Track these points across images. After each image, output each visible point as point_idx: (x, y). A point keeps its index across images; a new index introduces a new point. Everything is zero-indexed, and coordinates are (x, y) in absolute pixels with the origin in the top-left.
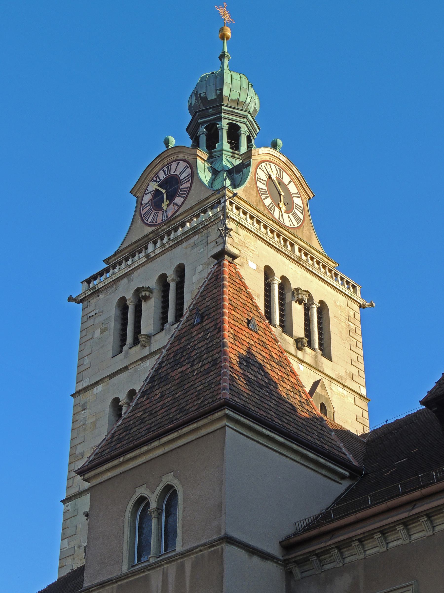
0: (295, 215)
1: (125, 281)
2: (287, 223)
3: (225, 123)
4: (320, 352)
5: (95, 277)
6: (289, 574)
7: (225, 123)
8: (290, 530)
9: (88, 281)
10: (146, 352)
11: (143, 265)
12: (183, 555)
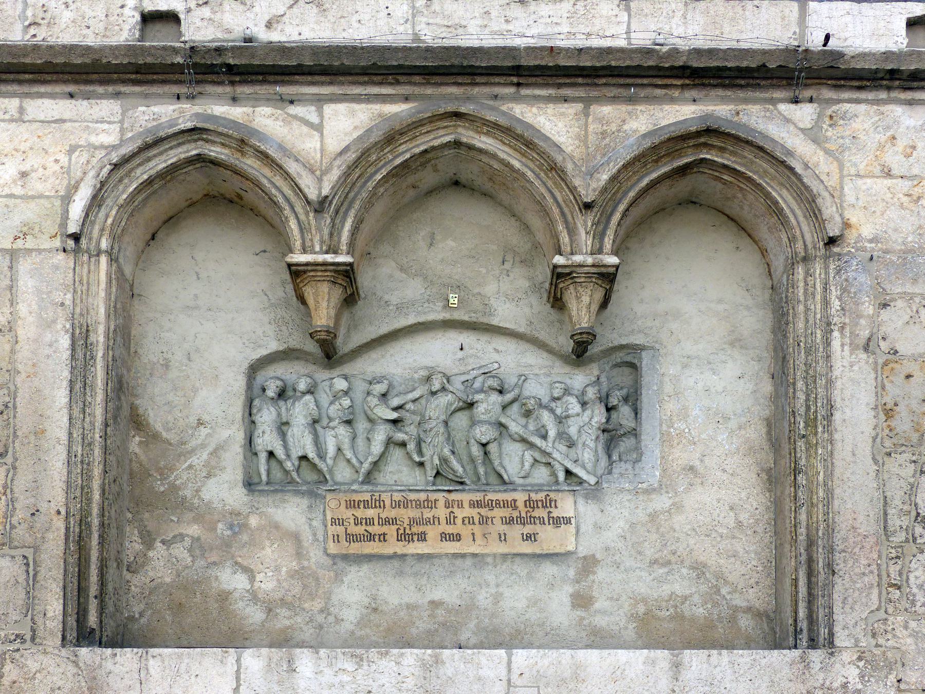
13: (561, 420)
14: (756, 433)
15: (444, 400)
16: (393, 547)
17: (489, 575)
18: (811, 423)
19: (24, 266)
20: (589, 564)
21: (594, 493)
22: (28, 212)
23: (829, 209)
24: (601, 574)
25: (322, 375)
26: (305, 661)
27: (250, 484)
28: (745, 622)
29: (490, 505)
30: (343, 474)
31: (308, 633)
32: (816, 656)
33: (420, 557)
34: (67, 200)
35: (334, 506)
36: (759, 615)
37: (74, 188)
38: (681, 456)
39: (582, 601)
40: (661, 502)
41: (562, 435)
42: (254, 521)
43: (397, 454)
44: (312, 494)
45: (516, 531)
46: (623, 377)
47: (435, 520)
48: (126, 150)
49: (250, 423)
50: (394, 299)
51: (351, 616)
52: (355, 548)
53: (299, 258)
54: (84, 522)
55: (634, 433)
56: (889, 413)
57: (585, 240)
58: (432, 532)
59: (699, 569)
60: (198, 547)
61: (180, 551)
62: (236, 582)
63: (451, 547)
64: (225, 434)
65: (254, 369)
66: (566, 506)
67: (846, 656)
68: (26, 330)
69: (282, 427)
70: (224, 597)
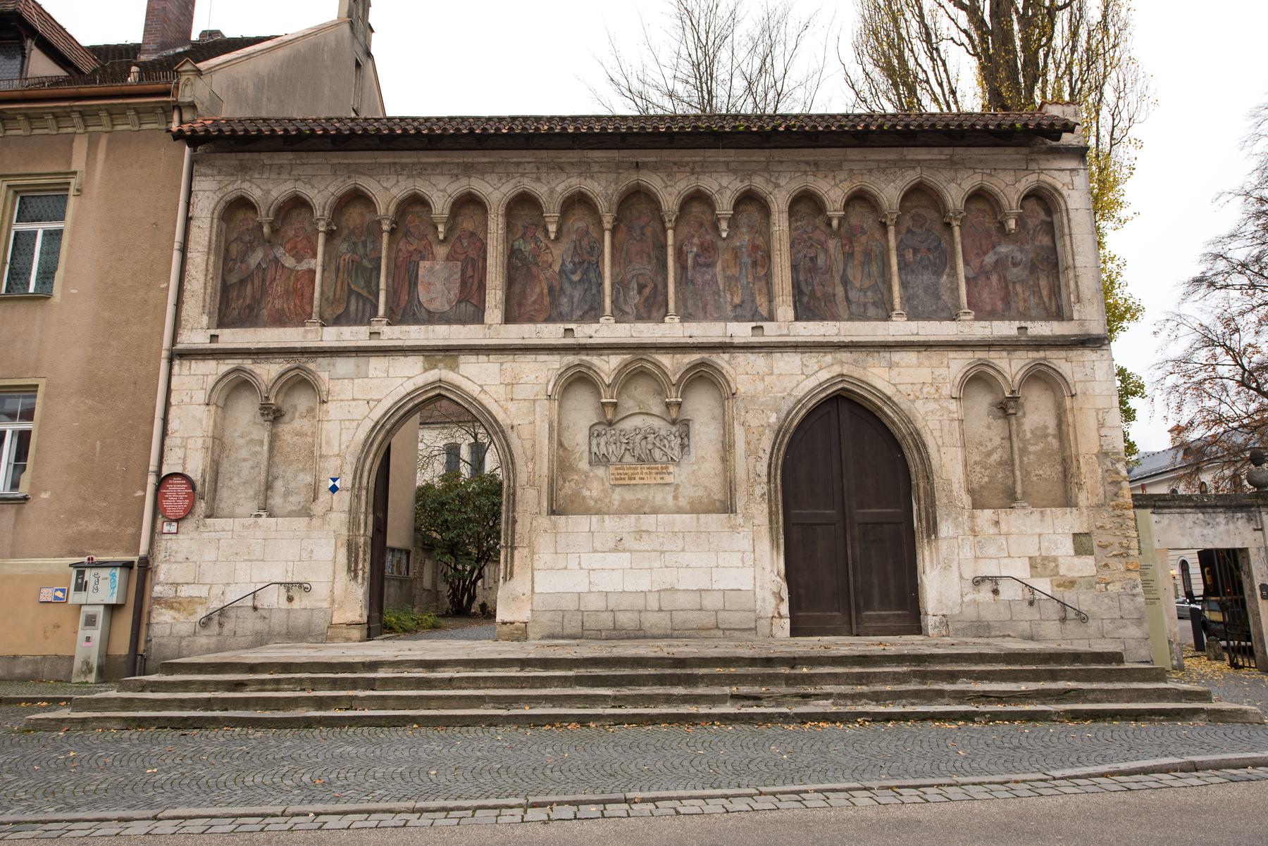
13: (669, 442)
14: (719, 446)
15: (639, 436)
16: (627, 482)
17: (652, 490)
18: (730, 446)
19: (537, 404)
20: (677, 486)
21: (678, 464)
22: (538, 388)
23: (733, 385)
24: (681, 489)
25: (608, 429)
26: (606, 517)
27: (590, 463)
28: (718, 504)
29: (652, 469)
30: (613, 459)
31: (605, 509)
32: (732, 515)
33: (634, 485)
34: (547, 384)
35: (612, 469)
36: (721, 502)
37: (549, 381)
39: (675, 498)
40: (695, 467)
41: (670, 446)
42: (591, 474)
43: (627, 452)
44: (606, 466)
45: (658, 477)
46: (685, 428)
47: (637, 474)
48: (562, 370)
49: (590, 444)
50: (626, 406)
51: (616, 503)
52: (617, 482)
53: (604, 400)
54: (553, 479)
55: (688, 446)
56: (749, 444)
57: (674, 394)
58: (637, 477)
59: (706, 487)
60: (577, 483)
61: (572, 484)
62: (586, 493)
63: (642, 482)
64: (583, 448)
65: (591, 428)
66: (671, 469)
67: (740, 516)
68: (538, 422)
69: (598, 444)
70: (584, 498)
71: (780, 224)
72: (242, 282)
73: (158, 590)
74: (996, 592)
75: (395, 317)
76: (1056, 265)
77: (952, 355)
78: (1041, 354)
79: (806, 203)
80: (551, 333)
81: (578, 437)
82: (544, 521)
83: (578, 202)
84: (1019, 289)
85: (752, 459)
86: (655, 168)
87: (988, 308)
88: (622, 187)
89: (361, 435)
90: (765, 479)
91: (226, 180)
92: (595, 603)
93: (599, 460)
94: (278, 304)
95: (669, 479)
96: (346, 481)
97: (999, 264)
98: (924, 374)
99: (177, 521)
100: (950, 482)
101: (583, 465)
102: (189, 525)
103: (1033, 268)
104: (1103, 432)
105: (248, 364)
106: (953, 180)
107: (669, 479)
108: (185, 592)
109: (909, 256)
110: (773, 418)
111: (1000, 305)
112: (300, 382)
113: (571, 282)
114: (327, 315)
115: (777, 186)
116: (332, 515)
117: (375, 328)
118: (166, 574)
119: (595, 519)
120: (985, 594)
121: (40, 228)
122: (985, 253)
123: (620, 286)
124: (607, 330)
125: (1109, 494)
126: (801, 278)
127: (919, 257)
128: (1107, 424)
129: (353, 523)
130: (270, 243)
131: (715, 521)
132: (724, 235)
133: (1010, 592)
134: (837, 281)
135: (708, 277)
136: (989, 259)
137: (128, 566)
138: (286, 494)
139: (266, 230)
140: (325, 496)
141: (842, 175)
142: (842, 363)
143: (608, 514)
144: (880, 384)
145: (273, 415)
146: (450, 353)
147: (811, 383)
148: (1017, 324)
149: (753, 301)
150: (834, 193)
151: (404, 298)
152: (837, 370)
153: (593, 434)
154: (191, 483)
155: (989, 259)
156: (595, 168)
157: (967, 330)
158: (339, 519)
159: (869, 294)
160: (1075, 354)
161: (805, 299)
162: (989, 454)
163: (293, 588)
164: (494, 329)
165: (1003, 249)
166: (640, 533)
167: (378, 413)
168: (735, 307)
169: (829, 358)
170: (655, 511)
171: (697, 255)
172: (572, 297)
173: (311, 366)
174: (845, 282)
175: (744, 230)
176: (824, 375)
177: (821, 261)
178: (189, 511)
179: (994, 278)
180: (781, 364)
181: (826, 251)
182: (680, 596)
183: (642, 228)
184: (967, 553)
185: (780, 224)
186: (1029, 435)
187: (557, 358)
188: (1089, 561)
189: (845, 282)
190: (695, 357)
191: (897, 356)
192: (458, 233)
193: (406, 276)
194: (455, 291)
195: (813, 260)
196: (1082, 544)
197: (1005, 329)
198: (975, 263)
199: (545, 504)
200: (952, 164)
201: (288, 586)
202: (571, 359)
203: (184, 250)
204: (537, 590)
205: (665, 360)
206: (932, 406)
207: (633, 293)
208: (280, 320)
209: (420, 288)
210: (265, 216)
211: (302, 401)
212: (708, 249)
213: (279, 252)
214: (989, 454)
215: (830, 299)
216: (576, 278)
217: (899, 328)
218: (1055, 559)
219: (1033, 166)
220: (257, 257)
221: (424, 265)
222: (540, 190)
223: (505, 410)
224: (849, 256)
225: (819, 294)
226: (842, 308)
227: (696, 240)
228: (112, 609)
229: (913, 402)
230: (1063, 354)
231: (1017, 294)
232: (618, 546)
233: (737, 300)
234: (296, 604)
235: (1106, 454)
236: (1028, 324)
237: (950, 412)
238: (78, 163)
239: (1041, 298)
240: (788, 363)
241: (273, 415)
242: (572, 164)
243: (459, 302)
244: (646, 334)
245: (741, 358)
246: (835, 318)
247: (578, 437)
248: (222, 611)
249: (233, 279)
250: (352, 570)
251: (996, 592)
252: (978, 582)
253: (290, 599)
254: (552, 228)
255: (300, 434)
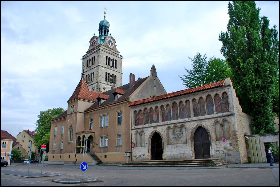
0: (113, 46)
1: (88, 57)
2: (111, 47)
3: (103, 30)
4: (115, 68)
5: (84, 56)
6: (85, 114)
7: (103, 30)
8: (86, 109)
9: (83, 56)
10: (90, 69)
11: (90, 55)
12: (74, 113)
38: (184, 136)
51: (175, 143)
62: (172, 142)
66: (181, 138)
71: (191, 104)
72: (137, 120)
73: (133, 155)
74: (219, 152)
75: (151, 123)
76: (228, 103)
77: (213, 119)
78: (225, 117)
79: (194, 100)
80: (166, 123)
81: (170, 135)
82: (166, 146)
83: (168, 105)
84: (224, 107)
85: (188, 137)
86: (176, 99)
87: (219, 111)
88: (172, 102)
89: (148, 137)
90: (190, 139)
91: (134, 109)
92: (172, 155)
93: (173, 138)
94: (140, 122)
95: (181, 139)
96: (147, 142)
97: (221, 104)
98: (209, 122)
99: (133, 147)
100: (213, 137)
101: (171, 139)
102: (134, 148)
103: (226, 104)
104: (234, 128)
105: (138, 130)
106: (212, 93)
107: (181, 139)
108: (135, 155)
109: (209, 105)
110: (191, 131)
111: (221, 110)
112: (142, 131)
113: (169, 115)
114: (145, 123)
115: (190, 99)
116: (146, 146)
117: (149, 124)
118: (133, 153)
119: (172, 145)
120: (218, 153)
121: (120, 116)
122: (219, 103)
123: (174, 115)
124: (172, 121)
125: (234, 137)
126: (195, 110)
127: (210, 105)
128: (234, 127)
129: (148, 147)
130: (139, 115)
131: (184, 145)
132: (185, 106)
133: (221, 152)
134: (200, 110)
135: (184, 112)
136: (219, 103)
137: (130, 152)
138: (143, 144)
139: (138, 114)
140: (146, 144)
141: (198, 96)
142: (199, 122)
143: (173, 144)
144: (203, 125)
145: (141, 135)
146: (155, 127)
147: (195, 126)
148: (221, 113)
149: (189, 115)
150: (197, 98)
151: (152, 120)
152: (198, 123)
153: (172, 134)
154: (134, 144)
155: (219, 103)
156: (169, 100)
157: (215, 115)
158: (147, 147)
159: (204, 111)
160: (229, 117)
161: (196, 113)
162: (220, 133)
163: (144, 155)
164: (160, 123)
165: (221, 102)
166: (177, 147)
167: (150, 134)
168: (187, 116)
169: (197, 122)
170: (179, 144)
171: (182, 109)
172: (169, 117)
173: (143, 129)
174: (200, 110)
175: (188, 105)
176: (197, 124)
177: (197, 108)
178: (134, 146)
179: (220, 106)
180: (191, 123)
181: (198, 106)
182: (181, 154)
183: (176, 107)
184: (215, 147)
185: (191, 104)
186: (226, 129)
187: (166, 126)
188: (232, 147)
189: (200, 110)
190: (182, 124)
191: (206, 120)
192: (156, 111)
193: (152, 117)
194: (157, 119)
195: (196, 108)
196: (231, 145)
197: (220, 114)
198: (217, 104)
199: (166, 144)
200: (212, 91)
201: (143, 154)
202: (168, 126)
203: (131, 118)
204: (167, 154)
205: (178, 124)
206: (210, 127)
207: (175, 116)
208: (141, 124)
209: (153, 118)
210: (138, 113)
211: (143, 133)
212: (184, 108)
213: (140, 116)
214: (220, 133)
215: (199, 113)
216: (169, 115)
217: (206, 116)
218: (227, 147)
219: (223, 89)
220: (138, 117)
221: (153, 115)
222: (163, 104)
223: (162, 133)
224: (201, 106)
225: (197, 112)
226: (200, 114)
227: (182, 107)
228: (129, 157)
229: (208, 127)
230: (228, 117)
231: (223, 108)
232: (174, 149)
233: (187, 115)
234: (144, 156)
235: (234, 131)
236: (223, 113)
237: (213, 127)
238: (122, 109)
239: (227, 108)
240: (192, 123)
241: (141, 135)
242: (167, 100)
243: (157, 119)
244: (176, 121)
245: (187, 123)
246: (199, 116)
247: (170, 135)
248: (138, 157)
249: (136, 120)
250: (149, 152)
251: (219, 152)
252: (217, 151)
253: (144, 156)
254: (166, 109)
255: (143, 137)
